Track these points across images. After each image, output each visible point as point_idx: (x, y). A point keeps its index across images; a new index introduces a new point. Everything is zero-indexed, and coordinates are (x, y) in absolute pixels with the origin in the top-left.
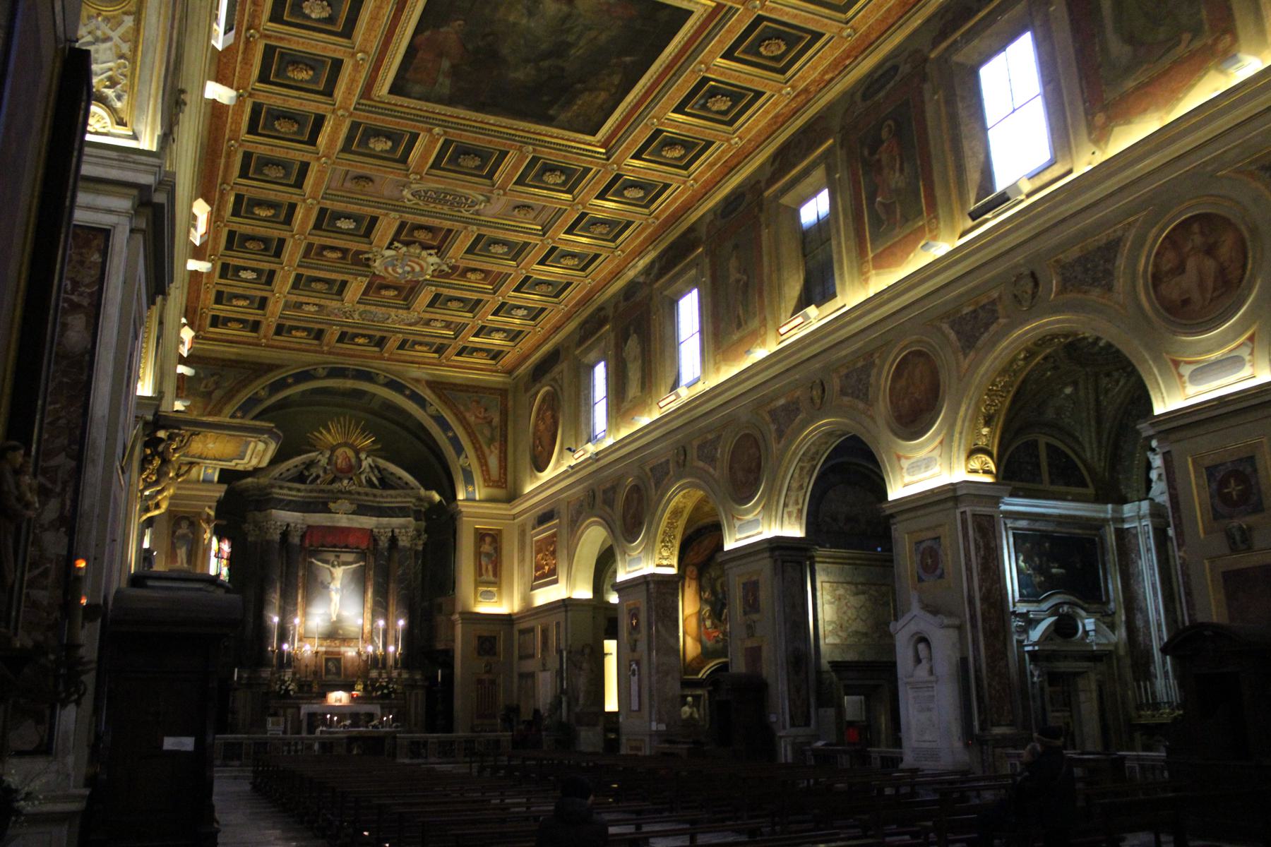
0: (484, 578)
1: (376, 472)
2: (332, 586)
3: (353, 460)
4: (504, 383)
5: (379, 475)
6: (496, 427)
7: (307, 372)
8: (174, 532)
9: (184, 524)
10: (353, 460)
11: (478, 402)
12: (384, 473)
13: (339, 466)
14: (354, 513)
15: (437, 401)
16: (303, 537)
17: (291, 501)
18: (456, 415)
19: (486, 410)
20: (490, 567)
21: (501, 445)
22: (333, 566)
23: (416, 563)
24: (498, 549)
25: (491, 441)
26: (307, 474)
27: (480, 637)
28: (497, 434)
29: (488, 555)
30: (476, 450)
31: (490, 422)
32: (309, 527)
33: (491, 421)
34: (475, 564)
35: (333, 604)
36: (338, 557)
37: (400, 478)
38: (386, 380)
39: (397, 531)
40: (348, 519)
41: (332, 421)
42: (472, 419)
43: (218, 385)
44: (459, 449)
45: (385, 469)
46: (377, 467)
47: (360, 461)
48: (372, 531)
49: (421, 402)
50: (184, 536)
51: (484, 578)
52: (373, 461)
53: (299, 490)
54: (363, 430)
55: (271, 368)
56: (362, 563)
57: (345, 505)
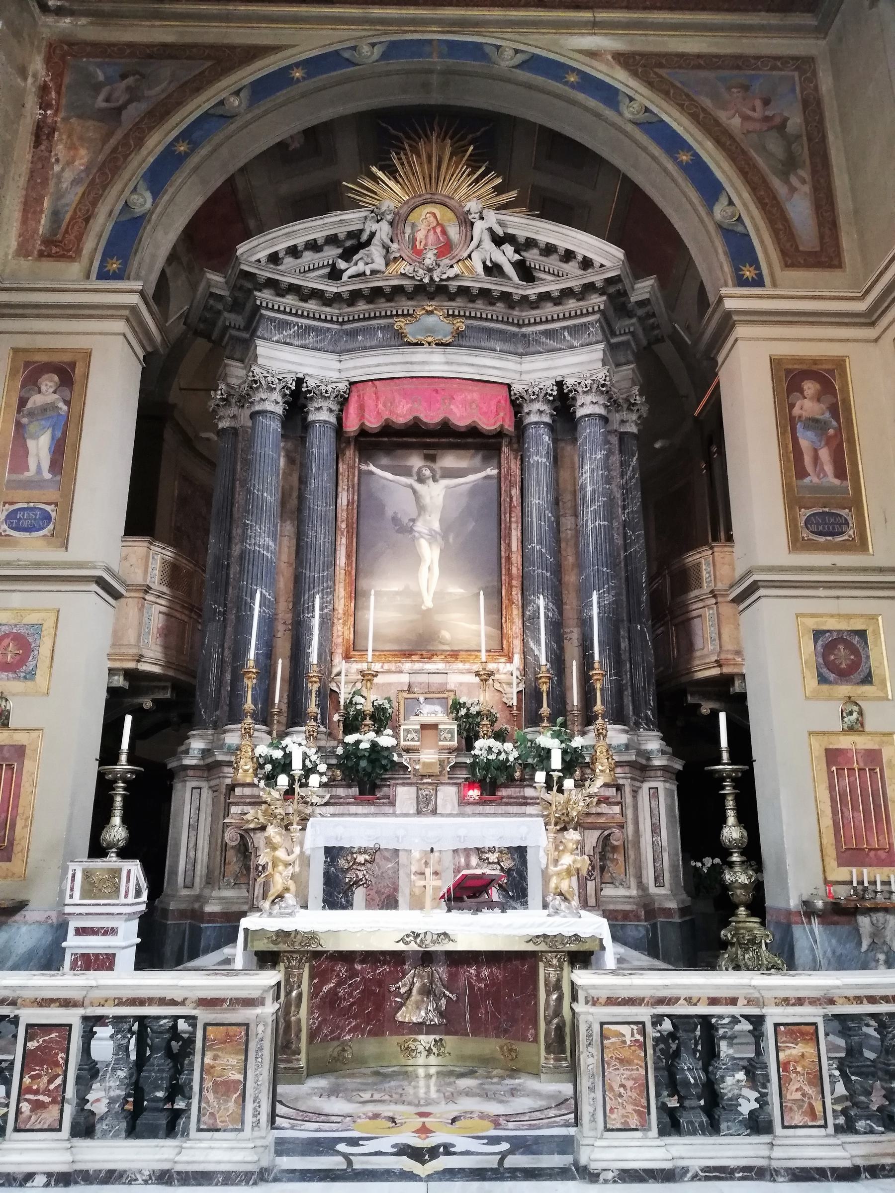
0: (812, 479)
2: (420, 527)
3: (454, 232)
6: (798, 137)
7: (337, 53)
8: (23, 402)
9: (49, 383)
11: (746, 88)
14: (459, 340)
16: (343, 401)
17: (309, 329)
18: (695, 117)
19: (766, 102)
20: (824, 454)
21: (814, 172)
22: (421, 480)
25: (789, 166)
26: (342, 265)
27: (818, 634)
28: (803, 152)
30: (754, 189)
31: (782, 127)
34: (782, 444)
35: (424, 569)
36: (432, 458)
38: (520, 58)
43: (134, 95)
45: (530, 243)
46: (510, 239)
50: (45, 409)
51: (812, 479)
55: (253, 53)
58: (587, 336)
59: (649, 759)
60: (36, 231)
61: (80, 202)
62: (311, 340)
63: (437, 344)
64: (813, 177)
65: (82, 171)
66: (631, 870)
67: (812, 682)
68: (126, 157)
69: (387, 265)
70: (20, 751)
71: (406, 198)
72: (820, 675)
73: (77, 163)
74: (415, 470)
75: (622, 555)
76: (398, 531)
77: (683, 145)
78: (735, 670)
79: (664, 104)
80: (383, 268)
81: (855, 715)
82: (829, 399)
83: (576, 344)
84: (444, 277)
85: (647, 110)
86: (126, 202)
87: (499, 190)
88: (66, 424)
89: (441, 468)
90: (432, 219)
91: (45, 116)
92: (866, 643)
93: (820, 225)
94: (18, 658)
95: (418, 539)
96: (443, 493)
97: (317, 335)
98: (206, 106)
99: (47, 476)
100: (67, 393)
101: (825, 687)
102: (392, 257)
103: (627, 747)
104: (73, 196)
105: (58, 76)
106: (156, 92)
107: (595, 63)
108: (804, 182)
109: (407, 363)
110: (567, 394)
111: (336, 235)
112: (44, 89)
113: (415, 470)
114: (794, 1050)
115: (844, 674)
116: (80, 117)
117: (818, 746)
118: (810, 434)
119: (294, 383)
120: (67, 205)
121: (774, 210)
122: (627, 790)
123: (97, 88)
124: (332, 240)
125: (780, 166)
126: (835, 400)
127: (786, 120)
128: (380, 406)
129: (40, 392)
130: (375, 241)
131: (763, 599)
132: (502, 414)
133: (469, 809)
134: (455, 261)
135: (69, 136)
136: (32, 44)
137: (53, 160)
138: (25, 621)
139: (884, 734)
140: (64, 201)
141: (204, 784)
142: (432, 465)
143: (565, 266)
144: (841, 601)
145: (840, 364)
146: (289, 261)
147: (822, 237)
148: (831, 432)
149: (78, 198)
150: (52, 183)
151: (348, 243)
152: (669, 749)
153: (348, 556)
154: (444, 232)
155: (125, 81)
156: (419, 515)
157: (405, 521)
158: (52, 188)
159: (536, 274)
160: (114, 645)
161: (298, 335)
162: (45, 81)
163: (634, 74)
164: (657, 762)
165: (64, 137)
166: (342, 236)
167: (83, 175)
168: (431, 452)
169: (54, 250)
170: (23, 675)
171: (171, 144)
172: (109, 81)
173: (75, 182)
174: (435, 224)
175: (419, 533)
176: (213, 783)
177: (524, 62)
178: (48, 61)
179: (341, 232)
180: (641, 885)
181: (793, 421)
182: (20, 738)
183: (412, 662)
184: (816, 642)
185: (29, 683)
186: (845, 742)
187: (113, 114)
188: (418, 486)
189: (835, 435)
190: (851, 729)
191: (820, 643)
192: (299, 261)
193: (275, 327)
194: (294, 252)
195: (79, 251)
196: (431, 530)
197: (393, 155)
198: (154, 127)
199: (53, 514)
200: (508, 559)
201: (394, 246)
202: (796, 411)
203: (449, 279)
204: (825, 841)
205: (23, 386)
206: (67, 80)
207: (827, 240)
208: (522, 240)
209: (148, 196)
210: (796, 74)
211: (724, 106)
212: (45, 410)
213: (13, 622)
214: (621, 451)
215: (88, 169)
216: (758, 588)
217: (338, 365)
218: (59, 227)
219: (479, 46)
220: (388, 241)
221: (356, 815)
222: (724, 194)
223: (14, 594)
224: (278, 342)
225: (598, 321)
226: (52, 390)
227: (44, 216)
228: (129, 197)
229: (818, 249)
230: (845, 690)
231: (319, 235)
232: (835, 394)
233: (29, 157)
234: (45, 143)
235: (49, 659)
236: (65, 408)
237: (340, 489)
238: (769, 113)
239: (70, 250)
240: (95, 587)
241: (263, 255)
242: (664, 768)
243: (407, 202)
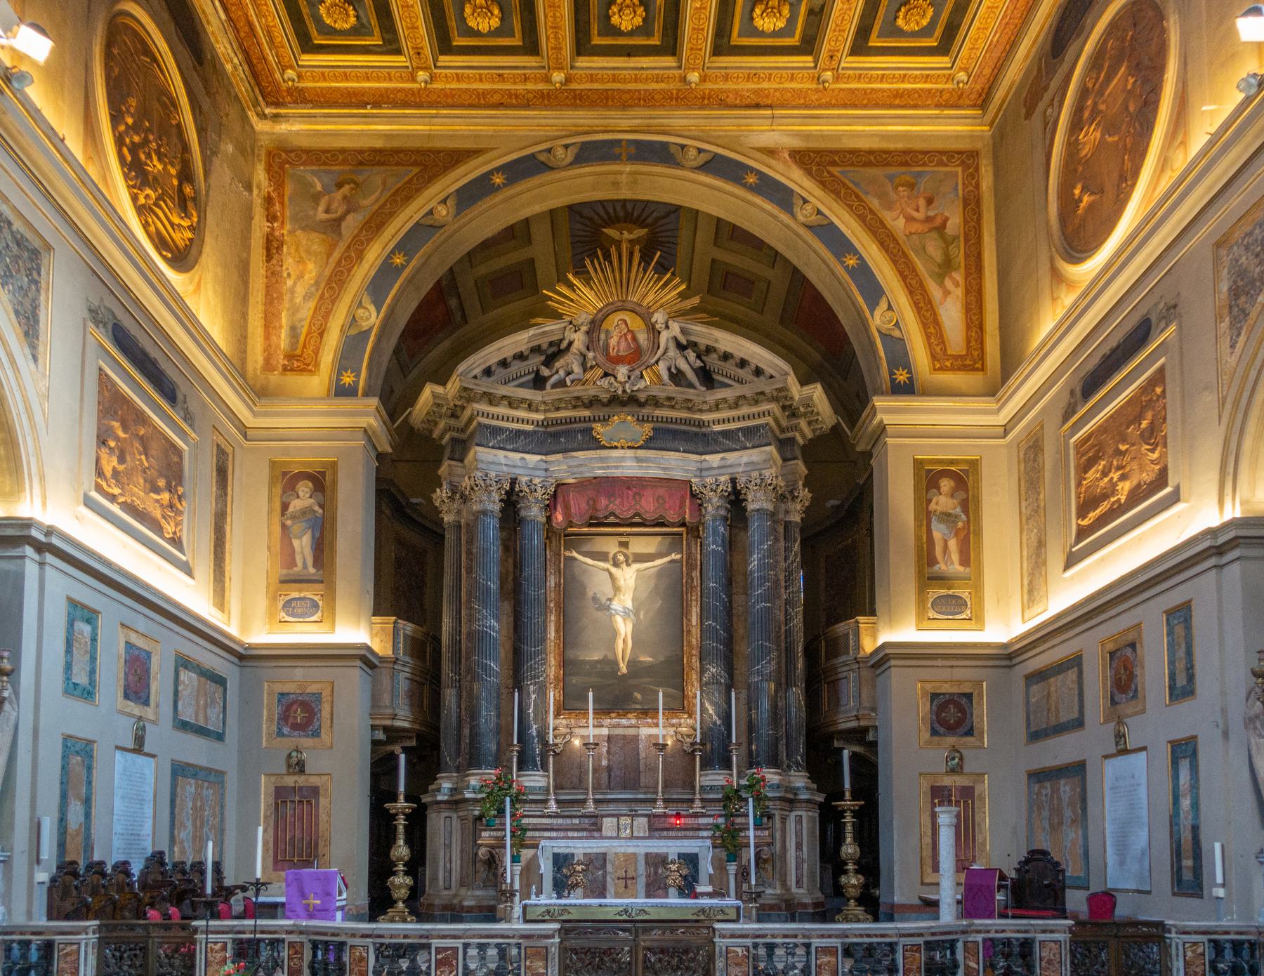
1: (691, 355)
2: (616, 605)
3: (643, 338)
4: (972, 137)
5: (699, 364)
6: (955, 238)
7: (533, 156)
8: (285, 507)
10: (643, 338)
11: (911, 186)
12: (712, 360)
13: (613, 353)
15: (818, 192)
18: (862, 218)
19: (930, 201)
20: (953, 544)
21: (967, 275)
24: (970, 504)
26: (545, 372)
27: (934, 696)
29: (947, 517)
30: (911, 292)
33: (943, 226)
37: (743, 363)
38: (703, 158)
39: (742, 480)
40: (638, 460)
41: (593, 255)
42: (898, 224)
44: (874, 292)
45: (709, 350)
46: (693, 345)
47: (654, 331)
49: (782, 196)
52: (683, 331)
53: (531, 407)
55: (456, 157)
57: (623, 426)
60: (278, 346)
61: (313, 317)
63: (629, 447)
64: (966, 279)
65: (312, 286)
66: (777, 876)
67: (926, 735)
68: (349, 270)
69: (585, 371)
70: (315, 791)
71: (600, 305)
72: (932, 729)
73: (306, 277)
74: (611, 556)
76: (598, 609)
77: (852, 250)
78: (870, 724)
79: (834, 205)
80: (581, 377)
81: (957, 760)
82: (961, 495)
83: (748, 445)
84: (635, 388)
85: (819, 212)
87: (683, 296)
88: (323, 525)
89: (634, 554)
90: (623, 326)
91: (273, 229)
92: (972, 703)
93: (968, 328)
94: (305, 720)
98: (417, 217)
99: (312, 570)
100: (320, 496)
101: (936, 738)
102: (589, 365)
103: (778, 786)
104: (307, 310)
105: (279, 186)
106: (369, 202)
107: (773, 162)
108: (957, 285)
111: (539, 346)
112: (268, 200)
113: (611, 556)
115: (951, 729)
116: (303, 229)
117: (925, 786)
118: (942, 526)
120: (301, 320)
121: (928, 315)
122: (777, 818)
123: (316, 198)
125: (937, 270)
126: (965, 496)
127: (946, 220)
129: (298, 497)
130: (574, 349)
131: (893, 669)
133: (657, 834)
134: (644, 367)
135: (297, 250)
136: (253, 153)
137: (285, 275)
138: (308, 691)
139: (978, 775)
140: (299, 316)
141: (454, 816)
143: (740, 371)
144: (955, 670)
145: (974, 465)
146: (500, 373)
147: (968, 341)
148: (960, 524)
149: (311, 312)
150: (286, 297)
152: (815, 786)
153: (557, 631)
154: (634, 339)
155: (342, 190)
156: (615, 595)
157: (603, 600)
158: (286, 304)
159: (716, 377)
160: (373, 706)
162: (269, 193)
163: (809, 173)
164: (802, 797)
165: (292, 250)
167: (313, 289)
168: (624, 539)
169: (296, 364)
171: (389, 257)
172: (327, 190)
173: (307, 297)
174: (626, 331)
176: (461, 814)
177: (707, 163)
178: (269, 169)
179: (544, 342)
180: (784, 883)
181: (929, 515)
182: (314, 781)
183: (611, 718)
184: (932, 702)
185: (316, 739)
186: (947, 781)
187: (334, 226)
188: (613, 570)
189: (964, 527)
190: (953, 771)
191: (935, 703)
192: (509, 370)
194: (504, 363)
195: (317, 365)
196: (624, 608)
197: (588, 262)
198: (371, 239)
199: (320, 603)
200: (689, 632)
201: (590, 355)
202: (932, 507)
203: (638, 390)
204: (924, 854)
205: (284, 492)
206: (289, 189)
207: (973, 343)
209: (372, 308)
210: (960, 170)
211: (889, 206)
212: (305, 513)
213: (298, 691)
215: (317, 283)
216: (889, 659)
218: (298, 342)
219: (665, 145)
220: (584, 350)
221: (573, 838)
222: (884, 298)
223: (297, 670)
224: (493, 447)
226: (308, 495)
227: (283, 331)
229: (964, 353)
230: (950, 740)
231: (524, 348)
232: (967, 491)
233: (263, 272)
234: (276, 257)
236: (320, 511)
237: (548, 573)
238: (931, 213)
239: (308, 365)
240: (358, 663)
242: (809, 801)
243: (601, 310)
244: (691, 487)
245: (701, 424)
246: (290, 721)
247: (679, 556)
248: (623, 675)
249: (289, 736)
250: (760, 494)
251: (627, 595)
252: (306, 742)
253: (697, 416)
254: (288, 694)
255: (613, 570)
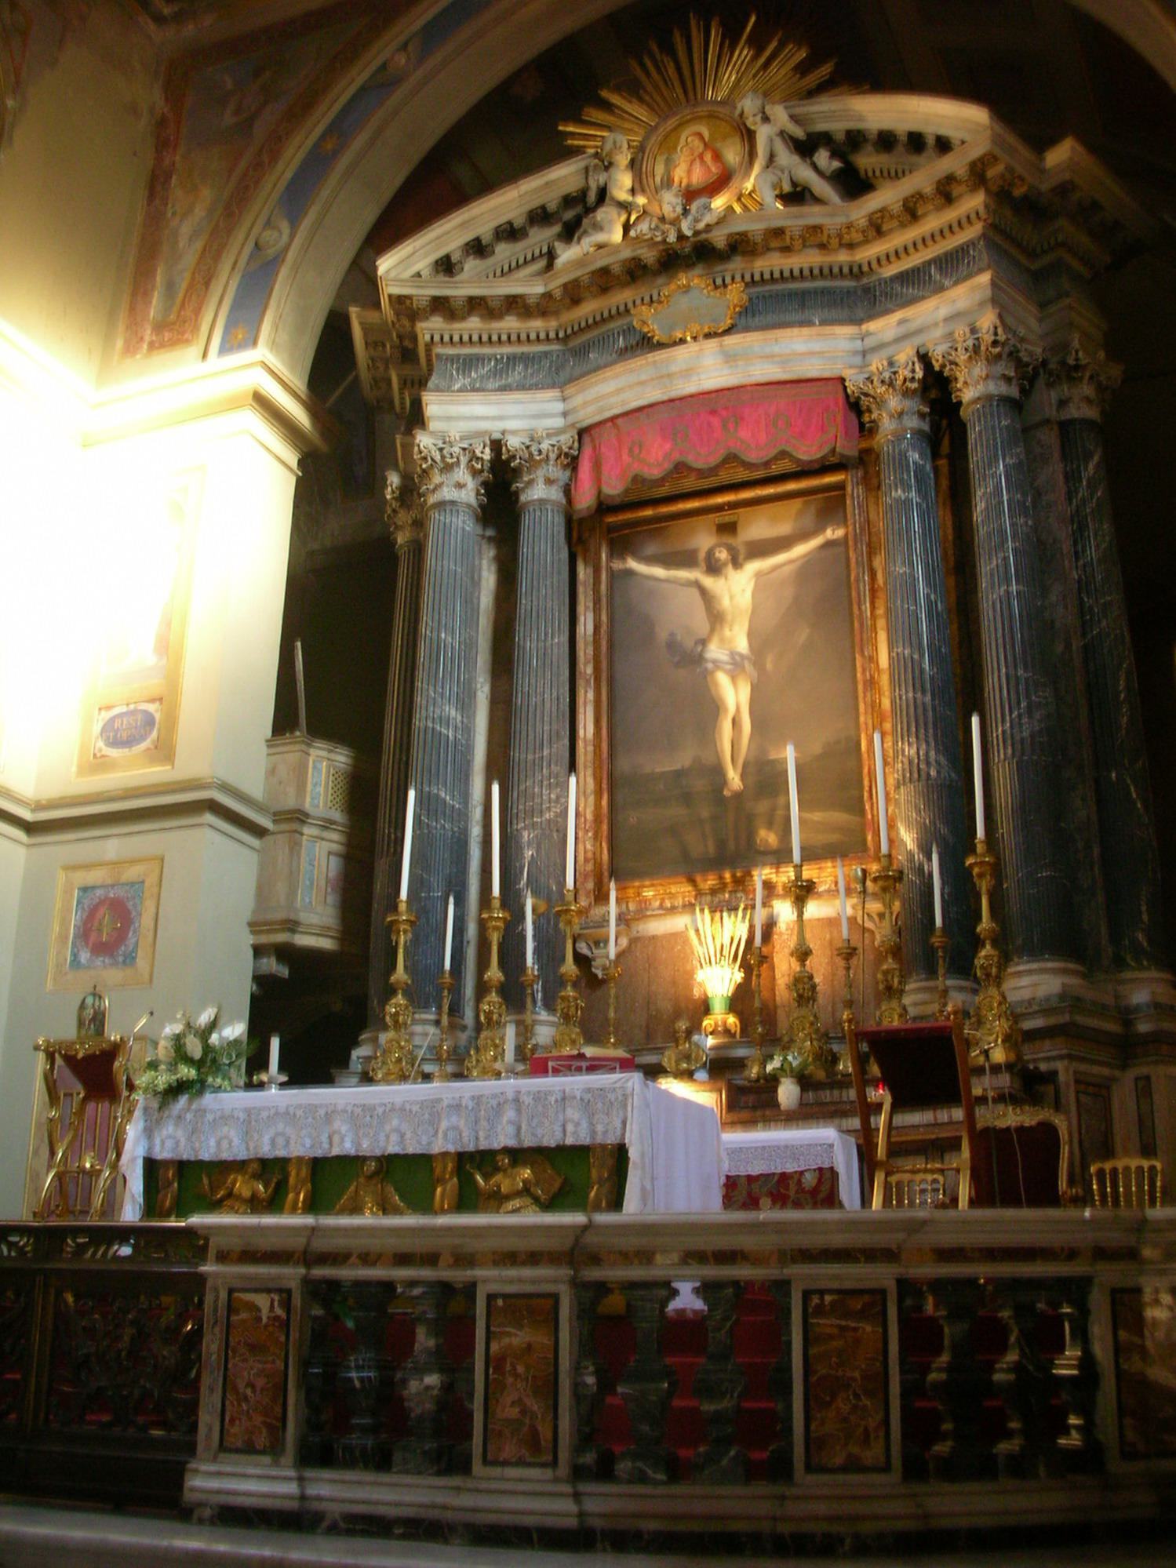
1: (822, 157)
2: (715, 651)
17: (513, 359)
22: (714, 568)
23: (1071, 477)
32: (581, 433)
36: (728, 529)
40: (730, 358)
45: (855, 139)
48: (842, 380)
52: (793, 118)
54: (757, 43)
56: (833, 533)
58: (965, 268)
59: (1128, 1023)
62: (517, 374)
63: (708, 336)
74: (702, 555)
75: (1076, 644)
76: (678, 665)
86: (256, 244)
95: (712, 673)
96: (752, 584)
97: (526, 367)
109: (662, 377)
110: (941, 372)
113: (702, 555)
114: (518, 1337)
119: (487, 450)
124: (540, 216)
128: (625, 457)
132: (832, 431)
142: (730, 540)
146: (472, 265)
151: (569, 215)
154: (717, 157)
156: (712, 630)
157: (689, 644)
161: (495, 373)
166: (552, 207)
168: (726, 517)
170: (121, 959)
173: (195, 235)
174: (701, 149)
175: (715, 662)
188: (708, 582)
192: (490, 261)
193: (458, 370)
196: (733, 654)
197: (634, 64)
199: (157, 716)
203: (709, 228)
208: (840, 137)
213: (109, 881)
214: (1064, 457)
217: (559, 407)
225: (984, 236)
228: (260, 234)
235: (151, 933)
241: (423, 264)
244: (845, 388)
245: (856, 272)
246: (93, 937)
247: (840, 533)
248: (738, 796)
249: (88, 968)
250: (979, 369)
251: (736, 628)
252: (111, 975)
253: (843, 257)
254: (93, 888)
255: (708, 582)
